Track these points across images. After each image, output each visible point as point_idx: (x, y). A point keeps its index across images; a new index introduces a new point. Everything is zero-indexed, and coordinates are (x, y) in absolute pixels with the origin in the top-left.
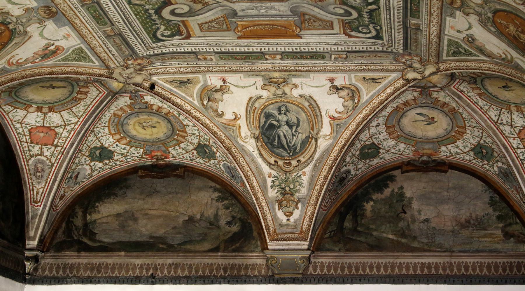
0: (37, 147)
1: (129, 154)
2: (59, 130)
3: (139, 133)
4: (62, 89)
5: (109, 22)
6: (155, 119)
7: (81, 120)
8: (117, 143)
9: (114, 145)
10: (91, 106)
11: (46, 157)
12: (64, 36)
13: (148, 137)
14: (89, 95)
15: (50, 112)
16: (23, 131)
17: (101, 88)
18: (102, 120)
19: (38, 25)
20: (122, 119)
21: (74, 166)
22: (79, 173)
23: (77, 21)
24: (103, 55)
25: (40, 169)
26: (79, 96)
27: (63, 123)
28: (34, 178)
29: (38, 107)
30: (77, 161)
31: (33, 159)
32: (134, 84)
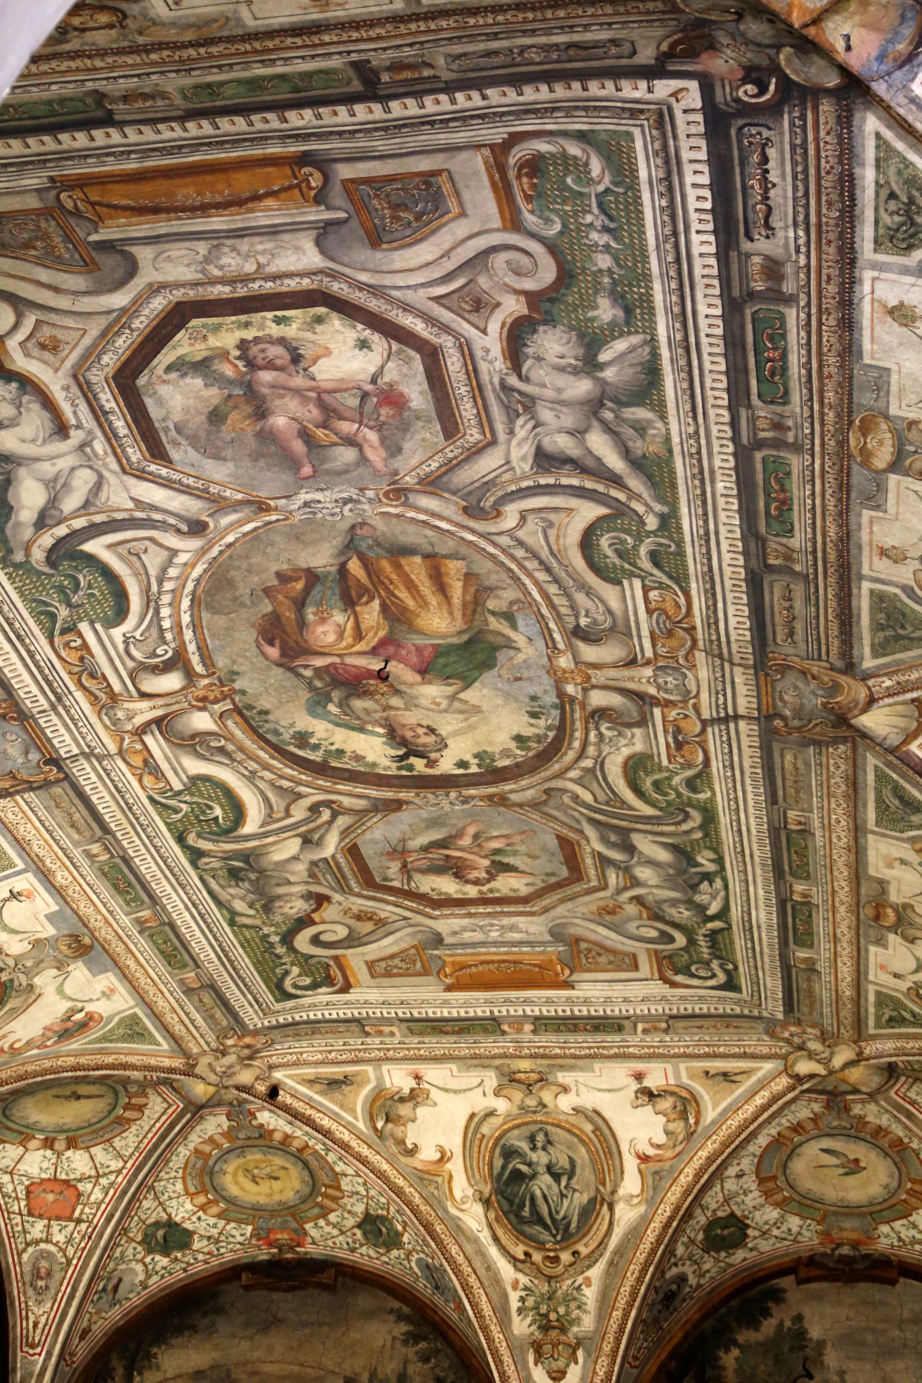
0: (40, 1224)
1: (222, 1238)
3: (242, 1189)
4: (94, 1101)
5: (191, 963)
6: (278, 1161)
7: (129, 1165)
8: (201, 1213)
9: (194, 1219)
10: (150, 1135)
11: (56, 1244)
12: (103, 993)
13: (262, 1200)
14: (147, 1112)
15: (68, 1148)
16: (15, 1190)
17: (172, 1097)
18: (171, 1164)
19: (55, 972)
20: (211, 1163)
21: (112, 1265)
22: (120, 1280)
23: (131, 963)
24: (178, 1029)
25: (43, 1272)
26: (128, 1114)
27: (93, 1173)
28: (30, 1292)
29: (46, 1139)
30: (117, 1254)
31: (30, 1250)
32: (238, 1088)
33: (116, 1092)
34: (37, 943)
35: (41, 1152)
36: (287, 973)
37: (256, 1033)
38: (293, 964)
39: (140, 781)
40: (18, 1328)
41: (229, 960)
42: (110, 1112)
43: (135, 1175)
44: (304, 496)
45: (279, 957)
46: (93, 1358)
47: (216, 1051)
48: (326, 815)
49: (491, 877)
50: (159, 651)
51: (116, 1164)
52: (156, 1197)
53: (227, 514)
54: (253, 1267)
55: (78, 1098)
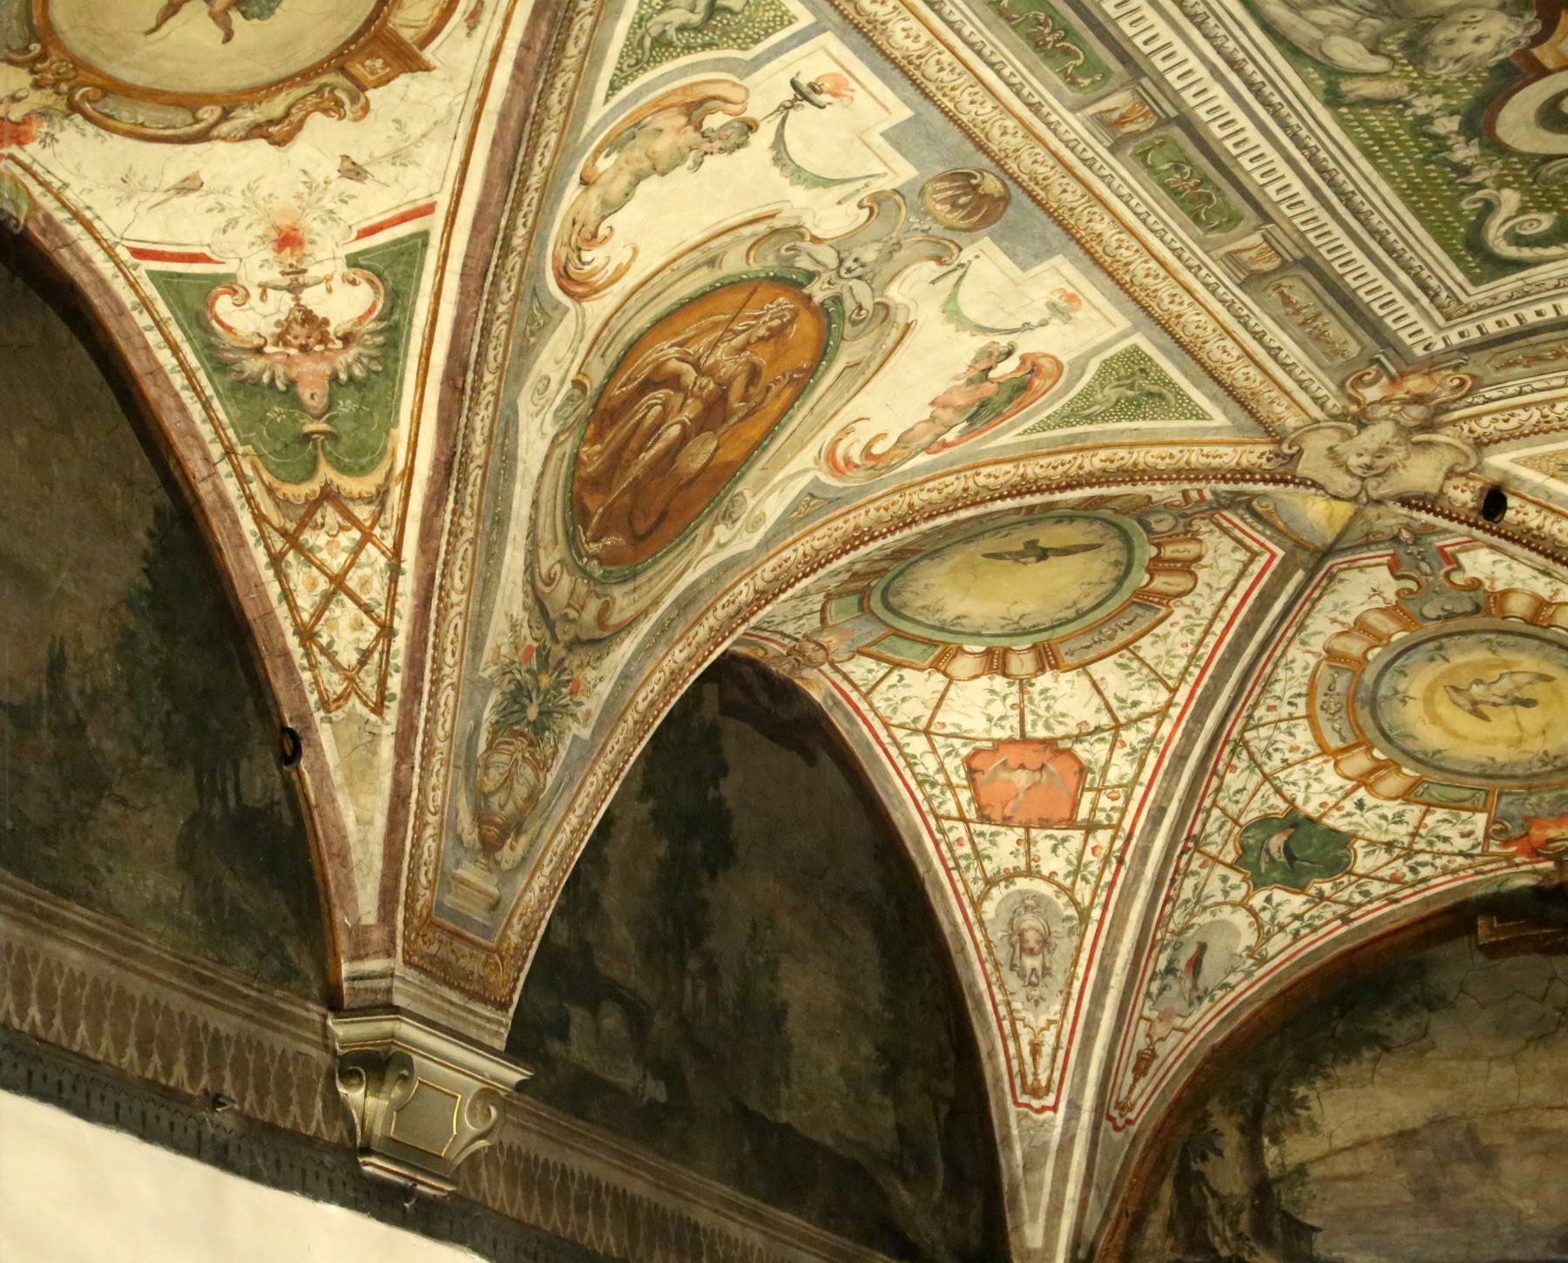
0: (1009, 839)
1: (1420, 844)
2: (1092, 752)
3: (1454, 734)
4: (1080, 557)
5: (1248, 211)
6: (1528, 662)
7: (1181, 696)
8: (1361, 793)
9: (1349, 805)
10: (1218, 627)
11: (1050, 879)
12: (1052, 306)
13: (1502, 753)
14: (1203, 575)
15: (1042, 670)
16: (941, 768)
17: (1256, 535)
18: (1278, 688)
19: (931, 269)
20: (1369, 677)
21: (1178, 918)
22: (1202, 948)
23: (1103, 226)
24: (1242, 375)
25: (1032, 938)
26: (1160, 583)
27: (1105, 720)
28: (1013, 982)
29: (989, 652)
30: (1187, 892)
31: (997, 893)
32: (1405, 501)
33: (1128, 532)
34: (876, 204)
35: (984, 681)
36: (1489, 208)
37: (1432, 364)
38: (1501, 184)
40: (999, 1057)
41: (1340, 193)
42: (1120, 581)
43: (1199, 719)
45: (1463, 170)
46: (1170, 1114)
47: (1342, 416)
51: (1151, 698)
52: (1255, 764)
54: (1501, 905)
55: (1043, 555)
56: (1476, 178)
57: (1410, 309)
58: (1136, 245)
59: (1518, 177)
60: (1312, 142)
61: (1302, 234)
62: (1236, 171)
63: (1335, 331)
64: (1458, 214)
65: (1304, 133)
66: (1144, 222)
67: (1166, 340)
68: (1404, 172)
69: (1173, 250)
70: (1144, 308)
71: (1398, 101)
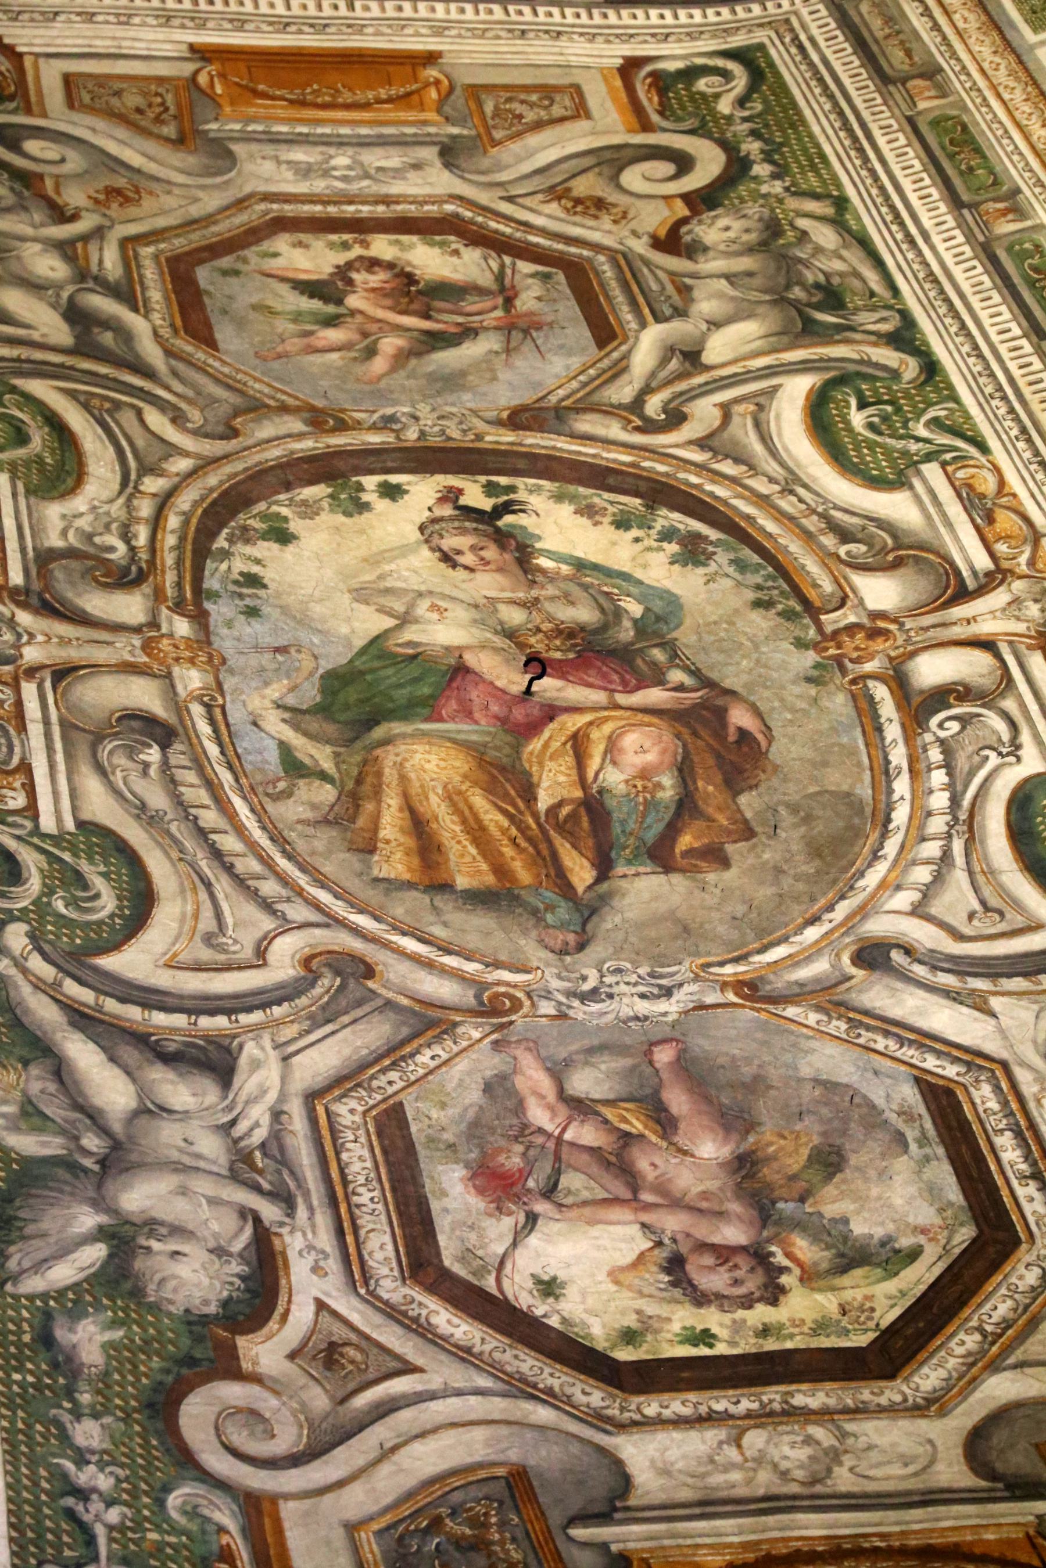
5: (924, 129)
36: (742, 102)
38: (729, 119)
39: (1002, 483)
41: (850, 131)
44: (671, 1007)
45: (755, 134)
48: (653, 406)
49: (343, 272)
50: (954, 726)
53: (817, 980)
56: (746, 126)
57: (815, 32)
58: (1017, 114)
59: (716, 122)
60: (864, 173)
61: (885, 103)
62: (926, 160)
63: (876, 24)
64: (765, 101)
65: (869, 181)
66: (1006, 131)
67: (1010, 34)
68: (799, 139)
69: (988, 106)
70: (1021, 62)
71: (794, 194)
